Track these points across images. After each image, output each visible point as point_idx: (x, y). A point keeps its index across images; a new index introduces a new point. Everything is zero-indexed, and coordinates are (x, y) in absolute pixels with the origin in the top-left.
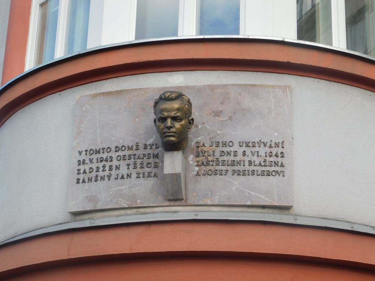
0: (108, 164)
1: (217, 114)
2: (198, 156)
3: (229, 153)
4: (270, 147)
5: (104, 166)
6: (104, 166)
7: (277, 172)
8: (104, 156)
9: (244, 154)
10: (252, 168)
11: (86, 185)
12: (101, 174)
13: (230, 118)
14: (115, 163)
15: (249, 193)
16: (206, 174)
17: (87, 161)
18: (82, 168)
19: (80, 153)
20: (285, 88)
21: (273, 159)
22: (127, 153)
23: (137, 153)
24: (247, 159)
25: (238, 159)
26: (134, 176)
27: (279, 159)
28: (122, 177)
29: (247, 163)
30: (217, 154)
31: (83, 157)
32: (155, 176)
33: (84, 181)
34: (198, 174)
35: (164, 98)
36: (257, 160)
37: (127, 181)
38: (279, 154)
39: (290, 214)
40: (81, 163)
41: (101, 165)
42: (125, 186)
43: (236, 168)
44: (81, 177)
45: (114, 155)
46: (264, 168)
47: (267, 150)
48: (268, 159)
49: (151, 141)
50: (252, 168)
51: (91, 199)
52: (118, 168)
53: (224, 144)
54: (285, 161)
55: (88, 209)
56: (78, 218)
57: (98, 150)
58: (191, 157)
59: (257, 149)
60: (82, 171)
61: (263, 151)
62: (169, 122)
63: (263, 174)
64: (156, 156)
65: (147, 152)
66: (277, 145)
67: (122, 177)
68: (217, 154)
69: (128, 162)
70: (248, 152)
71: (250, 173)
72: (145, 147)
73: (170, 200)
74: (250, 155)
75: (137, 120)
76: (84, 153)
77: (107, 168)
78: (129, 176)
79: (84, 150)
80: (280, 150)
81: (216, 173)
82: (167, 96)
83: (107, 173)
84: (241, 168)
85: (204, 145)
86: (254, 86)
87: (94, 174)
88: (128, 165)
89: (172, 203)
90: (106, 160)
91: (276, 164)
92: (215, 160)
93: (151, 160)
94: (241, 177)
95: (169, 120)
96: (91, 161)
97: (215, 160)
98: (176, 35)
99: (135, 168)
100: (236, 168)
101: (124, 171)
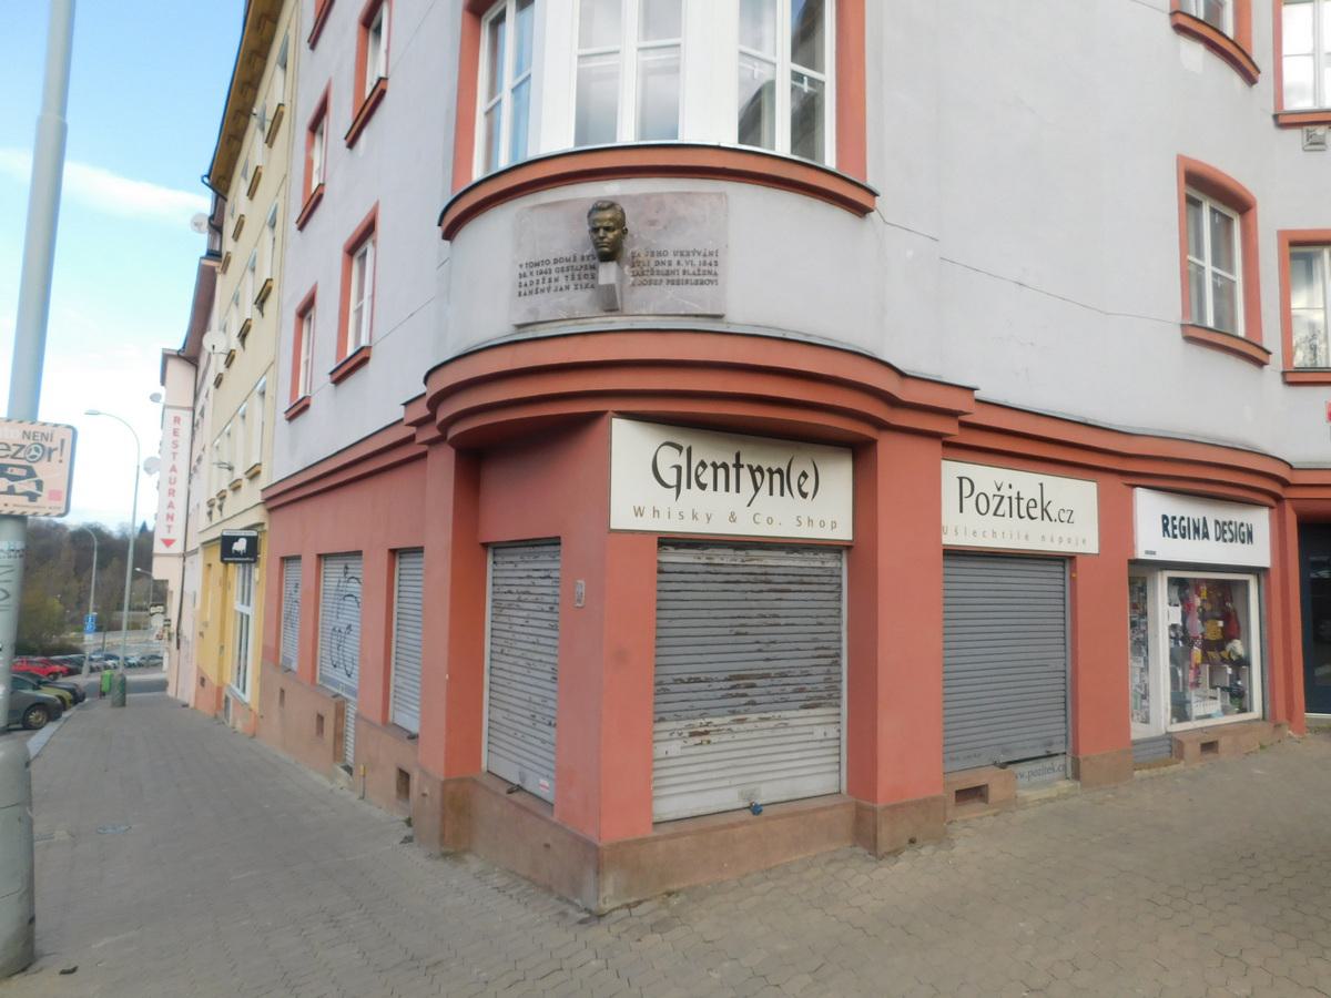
0: (547, 276)
1: (653, 223)
2: (633, 266)
3: (663, 263)
4: (705, 255)
5: (544, 279)
7: (709, 281)
8: (543, 268)
9: (678, 263)
10: (686, 277)
11: (527, 298)
12: (541, 286)
13: (665, 228)
14: (554, 275)
16: (642, 284)
17: (528, 274)
18: (523, 280)
19: (521, 266)
20: (720, 195)
21: (706, 268)
22: (565, 265)
23: (575, 264)
24: (681, 268)
25: (672, 268)
26: (572, 287)
27: (713, 268)
28: (561, 289)
29: (681, 273)
30: (652, 264)
31: (524, 270)
32: (593, 287)
33: (525, 294)
34: (633, 285)
35: (599, 207)
36: (691, 269)
37: (565, 292)
39: (723, 322)
41: (540, 277)
42: (563, 298)
43: (670, 278)
44: (523, 290)
45: (553, 267)
46: (698, 278)
47: (702, 258)
48: (703, 268)
49: (587, 253)
50: (686, 277)
51: (533, 311)
52: (556, 280)
53: (659, 254)
54: (718, 270)
56: (522, 330)
58: (627, 268)
59: (691, 258)
61: (697, 260)
62: (601, 233)
63: (696, 283)
65: (583, 263)
66: (711, 254)
67: (561, 289)
68: (652, 264)
69: (566, 273)
70: (682, 262)
72: (583, 258)
73: (606, 311)
77: (547, 281)
78: (568, 288)
80: (714, 258)
81: (650, 283)
83: (546, 285)
84: (675, 277)
85: (639, 255)
86: (689, 193)
87: (534, 287)
89: (609, 314)
90: (546, 273)
91: (710, 273)
94: (675, 286)
96: (531, 273)
98: (614, 140)
99: (573, 279)
100: (670, 278)
101: (562, 282)
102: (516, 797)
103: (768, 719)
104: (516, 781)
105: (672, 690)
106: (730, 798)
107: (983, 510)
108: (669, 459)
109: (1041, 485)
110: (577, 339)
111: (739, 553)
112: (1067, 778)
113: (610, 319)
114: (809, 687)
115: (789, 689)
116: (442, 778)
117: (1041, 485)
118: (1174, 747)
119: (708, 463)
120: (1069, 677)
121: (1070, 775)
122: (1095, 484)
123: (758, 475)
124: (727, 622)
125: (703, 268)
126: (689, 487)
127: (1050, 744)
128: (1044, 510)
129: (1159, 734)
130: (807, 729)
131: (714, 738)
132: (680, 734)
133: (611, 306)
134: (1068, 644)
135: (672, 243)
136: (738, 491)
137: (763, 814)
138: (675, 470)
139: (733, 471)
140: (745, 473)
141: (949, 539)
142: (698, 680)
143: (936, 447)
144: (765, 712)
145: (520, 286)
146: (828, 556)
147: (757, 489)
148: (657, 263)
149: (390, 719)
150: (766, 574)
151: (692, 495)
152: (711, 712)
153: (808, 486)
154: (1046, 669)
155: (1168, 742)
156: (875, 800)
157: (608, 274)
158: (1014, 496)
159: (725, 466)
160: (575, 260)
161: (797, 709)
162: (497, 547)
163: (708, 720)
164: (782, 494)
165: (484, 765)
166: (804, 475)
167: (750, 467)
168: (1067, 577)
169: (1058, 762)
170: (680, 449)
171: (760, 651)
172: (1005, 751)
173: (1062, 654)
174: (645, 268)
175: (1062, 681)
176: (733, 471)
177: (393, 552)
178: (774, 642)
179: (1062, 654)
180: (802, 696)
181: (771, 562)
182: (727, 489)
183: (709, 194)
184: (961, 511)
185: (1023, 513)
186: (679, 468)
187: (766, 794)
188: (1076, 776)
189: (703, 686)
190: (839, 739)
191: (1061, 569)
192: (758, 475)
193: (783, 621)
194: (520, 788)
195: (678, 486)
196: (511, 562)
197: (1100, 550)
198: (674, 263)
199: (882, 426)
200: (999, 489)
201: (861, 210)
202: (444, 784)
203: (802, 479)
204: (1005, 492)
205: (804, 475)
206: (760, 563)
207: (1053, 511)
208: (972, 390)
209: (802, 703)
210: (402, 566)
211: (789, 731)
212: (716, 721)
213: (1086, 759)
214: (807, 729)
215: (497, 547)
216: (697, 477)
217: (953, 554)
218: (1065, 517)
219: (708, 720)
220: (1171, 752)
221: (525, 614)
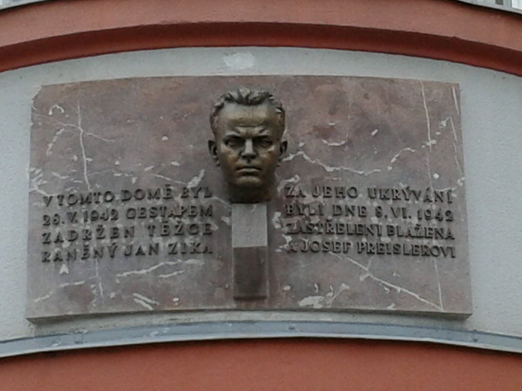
3: (350, 211)
4: (427, 200)
5: (100, 229)
6: (100, 229)
13: (349, 143)
15: (391, 288)
18: (54, 231)
19: (48, 201)
22: (148, 203)
29: (384, 231)
31: (55, 208)
34: (292, 251)
38: (443, 214)
40: (51, 221)
44: (54, 250)
45: (122, 208)
49: (194, 182)
52: (128, 233)
53: (341, 193)
55: (70, 313)
57: (85, 198)
59: (402, 204)
60: (53, 238)
62: (249, 148)
63: (415, 252)
64: (207, 212)
66: (439, 197)
70: (386, 211)
71: (392, 250)
74: (390, 215)
75: (165, 138)
76: (56, 201)
79: (55, 195)
82: (244, 95)
88: (151, 228)
89: (243, 305)
91: (439, 234)
92: (324, 223)
93: (196, 220)
95: (249, 144)
97: (324, 223)
145: (47, 243)
148: (338, 211)
174: (315, 220)
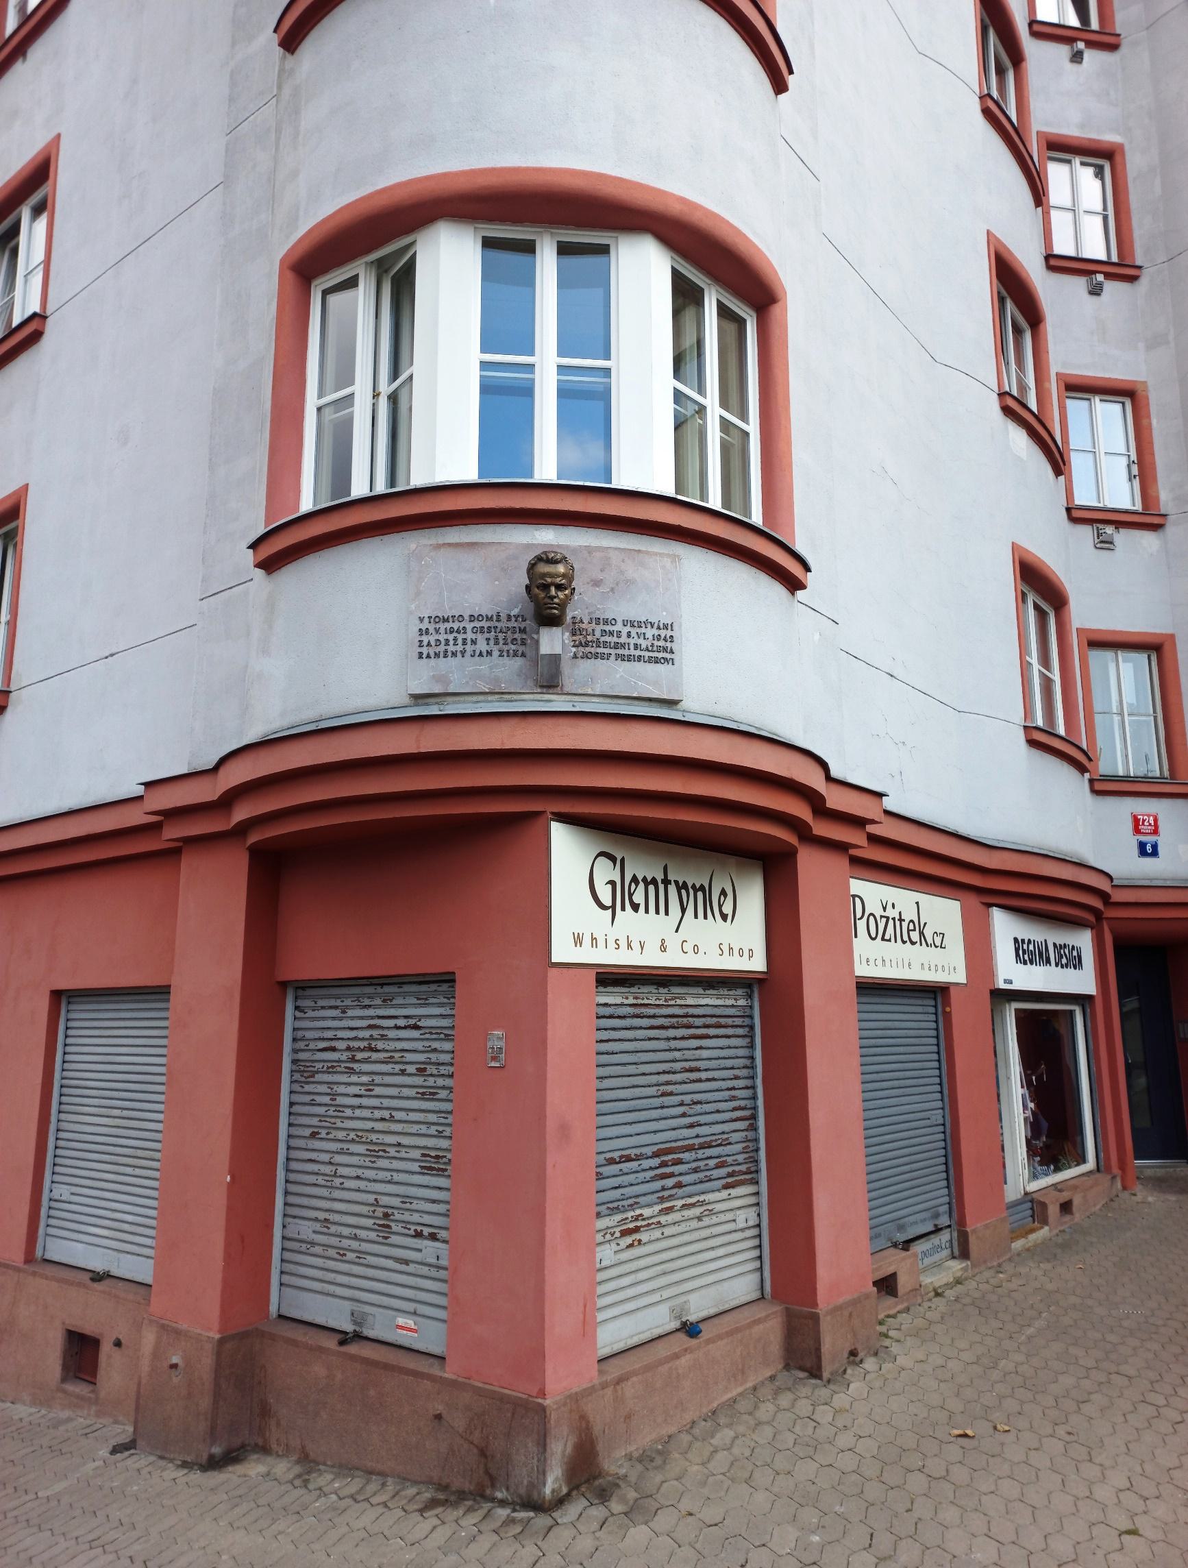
0: (460, 637)
1: (597, 583)
2: (573, 635)
3: (611, 633)
5: (455, 639)
6: (455, 639)
7: (666, 660)
8: (456, 626)
9: (629, 635)
10: (638, 653)
11: (433, 662)
12: (451, 648)
13: (612, 590)
14: (470, 636)
15: (635, 683)
16: (586, 656)
17: (431, 630)
18: (425, 639)
19: (421, 620)
20: (675, 558)
21: (661, 643)
22: (485, 624)
23: (499, 625)
24: (632, 641)
25: (622, 640)
26: (496, 653)
27: (669, 644)
28: (481, 654)
29: (632, 647)
30: (598, 634)
32: (523, 655)
33: (428, 656)
34: (575, 657)
35: (546, 558)
36: (644, 644)
37: (487, 659)
38: (668, 637)
39: (677, 710)
40: (424, 633)
41: (451, 637)
42: (484, 665)
43: (620, 652)
44: (425, 650)
45: (469, 626)
46: (651, 654)
47: (656, 632)
48: (656, 643)
49: (515, 612)
50: (638, 653)
51: (438, 679)
52: (474, 642)
53: (606, 622)
54: (675, 646)
55: (437, 691)
56: (420, 701)
57: (446, 617)
58: (567, 634)
59: (643, 630)
60: (425, 643)
61: (650, 632)
64: (523, 631)
65: (510, 625)
66: (666, 627)
67: (481, 654)
68: (598, 634)
69: (487, 635)
70: (633, 634)
71: (636, 659)
72: (509, 618)
73: (542, 687)
74: (636, 637)
75: (497, 583)
76: (426, 620)
77: (460, 641)
78: (489, 653)
79: (426, 616)
80: (669, 633)
81: (596, 656)
82: (550, 557)
83: (459, 648)
84: (626, 652)
85: (581, 621)
86: (639, 551)
87: (442, 648)
88: (488, 639)
89: (545, 690)
90: (458, 632)
91: (665, 650)
92: (595, 640)
93: (516, 636)
94: (626, 663)
95: (553, 589)
96: (437, 631)
97: (595, 640)
98: (532, 477)
99: (497, 643)
100: (620, 652)
101: (482, 646)
102: (353, 1349)
103: (693, 1205)
104: (349, 1327)
105: (605, 1174)
106: (659, 1320)
107: (873, 935)
108: (605, 872)
109: (917, 903)
110: (513, 722)
111: (662, 990)
112: (954, 1258)
113: (547, 697)
114: (729, 1159)
115: (712, 1163)
116: (217, 1336)
117: (917, 903)
118: (1035, 1208)
119: (640, 878)
120: (948, 1131)
121: (956, 1252)
122: (958, 903)
123: (683, 892)
124: (654, 1079)
125: (656, 643)
126: (623, 909)
127: (937, 1216)
128: (921, 933)
129: (1019, 1197)
130: (730, 1216)
131: (644, 1237)
132: (612, 1235)
133: (550, 680)
134: (946, 1092)
135: (622, 609)
136: (667, 913)
137: (705, 1335)
138: (609, 886)
139: (661, 887)
140: (672, 889)
141: (862, 970)
142: (628, 1159)
143: (844, 863)
144: (690, 1196)
145: (420, 646)
146: (645, 989)
147: (683, 910)
148: (604, 632)
149: (39, 1253)
150: (686, 1016)
151: (626, 916)
152: (641, 1200)
153: (727, 909)
154: (927, 1122)
155: (1029, 1204)
156: (815, 1305)
157: (552, 641)
158: (897, 917)
159: (654, 881)
160: (498, 620)
161: (719, 1190)
162: (302, 987)
163: (638, 1212)
164: (705, 917)
165: (273, 1309)
166: (723, 893)
167: (676, 882)
168: (940, 1009)
169: (945, 1236)
170: (613, 859)
171: (684, 1115)
172: (901, 1228)
173: (939, 1104)
174: (589, 638)
175: (941, 1136)
176: (661, 887)
177: (57, 996)
178: (700, 1103)
179: (939, 1104)
180: (723, 1172)
181: (690, 1001)
182: (657, 912)
183: (661, 555)
184: (677, 931)
185: (906, 938)
186: (612, 883)
187: (698, 1307)
188: (964, 1254)
189: (633, 1165)
190: (759, 1226)
191: (933, 1003)
192: (683, 892)
193: (703, 1075)
194: (358, 1337)
195: (613, 907)
196: (336, 1007)
197: (968, 977)
198: (624, 634)
199: (806, 835)
200: (885, 910)
201: (793, 584)
202: (221, 1342)
203: (722, 898)
204: (891, 913)
205: (723, 893)
206: (682, 1002)
207: (928, 933)
208: (880, 795)
209: (724, 1182)
210: (72, 1016)
211: (715, 1220)
212: (647, 1212)
213: (974, 1231)
214: (730, 1216)
215: (302, 987)
216: (631, 895)
217: (870, 988)
218: (938, 941)
219: (638, 1212)
220: (1032, 1216)
221: (365, 1079)
